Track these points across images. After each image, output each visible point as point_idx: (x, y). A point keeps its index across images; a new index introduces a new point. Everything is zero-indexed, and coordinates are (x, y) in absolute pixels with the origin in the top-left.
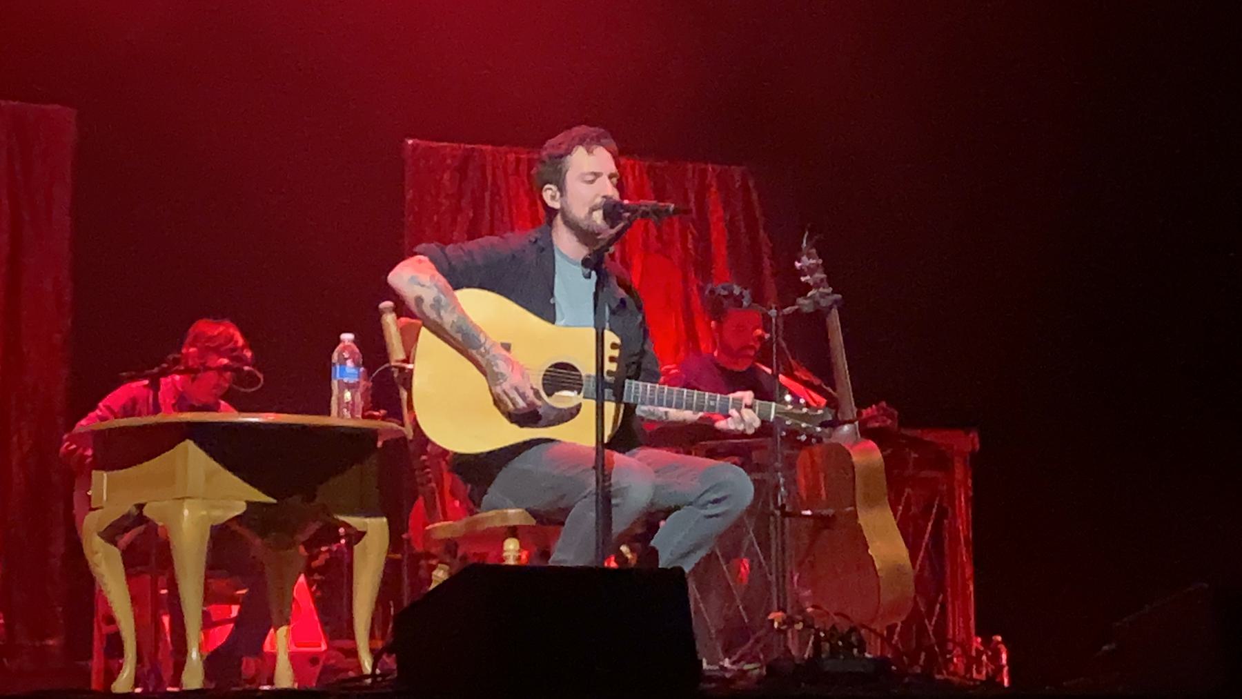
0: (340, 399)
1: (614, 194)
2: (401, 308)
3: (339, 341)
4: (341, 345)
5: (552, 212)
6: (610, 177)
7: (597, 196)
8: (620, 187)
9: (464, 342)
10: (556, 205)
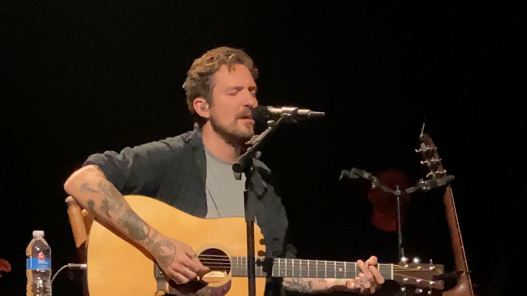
0: (34, 285)
1: (253, 102)
3: (31, 237)
4: (33, 241)
5: (202, 121)
6: (250, 89)
9: (131, 234)
10: (205, 114)
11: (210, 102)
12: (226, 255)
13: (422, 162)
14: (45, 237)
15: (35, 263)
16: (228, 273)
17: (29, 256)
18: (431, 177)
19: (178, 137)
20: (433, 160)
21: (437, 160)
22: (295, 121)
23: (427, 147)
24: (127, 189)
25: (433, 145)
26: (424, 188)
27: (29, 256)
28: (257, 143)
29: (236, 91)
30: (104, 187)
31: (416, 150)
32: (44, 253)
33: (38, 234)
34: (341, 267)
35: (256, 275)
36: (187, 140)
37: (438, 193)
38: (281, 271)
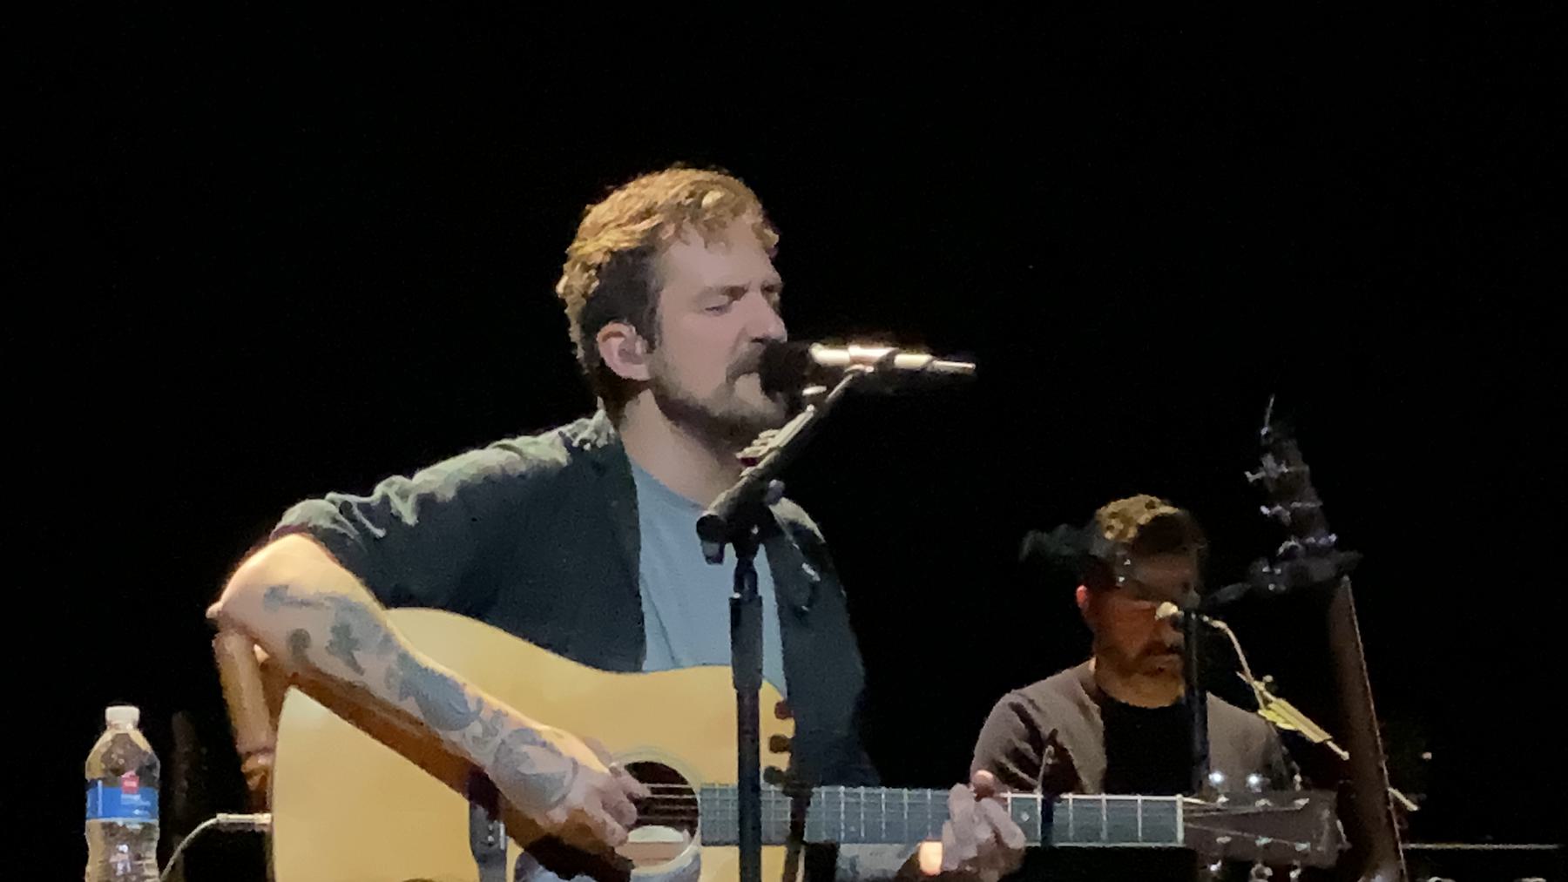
1: (776, 329)
3: (100, 726)
4: (107, 737)
7: (738, 341)
8: (786, 310)
11: (648, 331)
12: (683, 781)
13: (1264, 510)
14: (142, 725)
15: (113, 807)
16: (692, 834)
17: (94, 782)
18: (1290, 553)
19: (555, 433)
20: (1297, 505)
21: (1309, 505)
22: (889, 390)
23: (1279, 464)
25: (1295, 454)
26: (1271, 587)
27: (94, 782)
28: (773, 454)
29: (726, 299)
31: (1248, 474)
32: (139, 773)
33: (123, 718)
35: (763, 839)
36: (576, 443)
37: (1308, 601)
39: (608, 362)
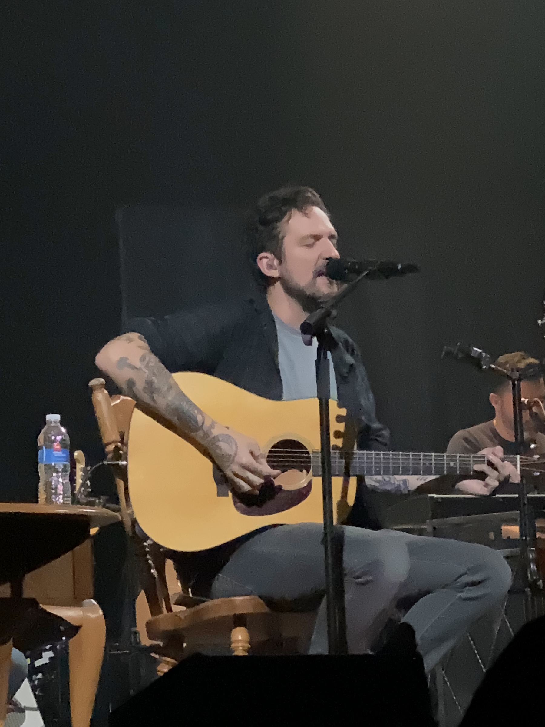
2: (113, 389)
9: (181, 423)
24: (173, 366)
30: (148, 363)
34: (452, 461)
38: (376, 467)
39: (263, 271)
